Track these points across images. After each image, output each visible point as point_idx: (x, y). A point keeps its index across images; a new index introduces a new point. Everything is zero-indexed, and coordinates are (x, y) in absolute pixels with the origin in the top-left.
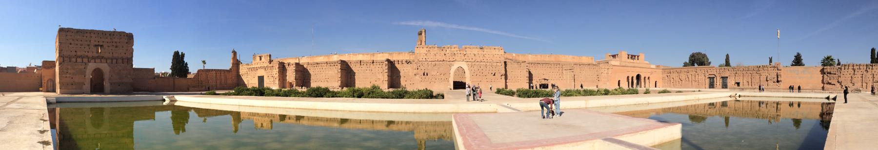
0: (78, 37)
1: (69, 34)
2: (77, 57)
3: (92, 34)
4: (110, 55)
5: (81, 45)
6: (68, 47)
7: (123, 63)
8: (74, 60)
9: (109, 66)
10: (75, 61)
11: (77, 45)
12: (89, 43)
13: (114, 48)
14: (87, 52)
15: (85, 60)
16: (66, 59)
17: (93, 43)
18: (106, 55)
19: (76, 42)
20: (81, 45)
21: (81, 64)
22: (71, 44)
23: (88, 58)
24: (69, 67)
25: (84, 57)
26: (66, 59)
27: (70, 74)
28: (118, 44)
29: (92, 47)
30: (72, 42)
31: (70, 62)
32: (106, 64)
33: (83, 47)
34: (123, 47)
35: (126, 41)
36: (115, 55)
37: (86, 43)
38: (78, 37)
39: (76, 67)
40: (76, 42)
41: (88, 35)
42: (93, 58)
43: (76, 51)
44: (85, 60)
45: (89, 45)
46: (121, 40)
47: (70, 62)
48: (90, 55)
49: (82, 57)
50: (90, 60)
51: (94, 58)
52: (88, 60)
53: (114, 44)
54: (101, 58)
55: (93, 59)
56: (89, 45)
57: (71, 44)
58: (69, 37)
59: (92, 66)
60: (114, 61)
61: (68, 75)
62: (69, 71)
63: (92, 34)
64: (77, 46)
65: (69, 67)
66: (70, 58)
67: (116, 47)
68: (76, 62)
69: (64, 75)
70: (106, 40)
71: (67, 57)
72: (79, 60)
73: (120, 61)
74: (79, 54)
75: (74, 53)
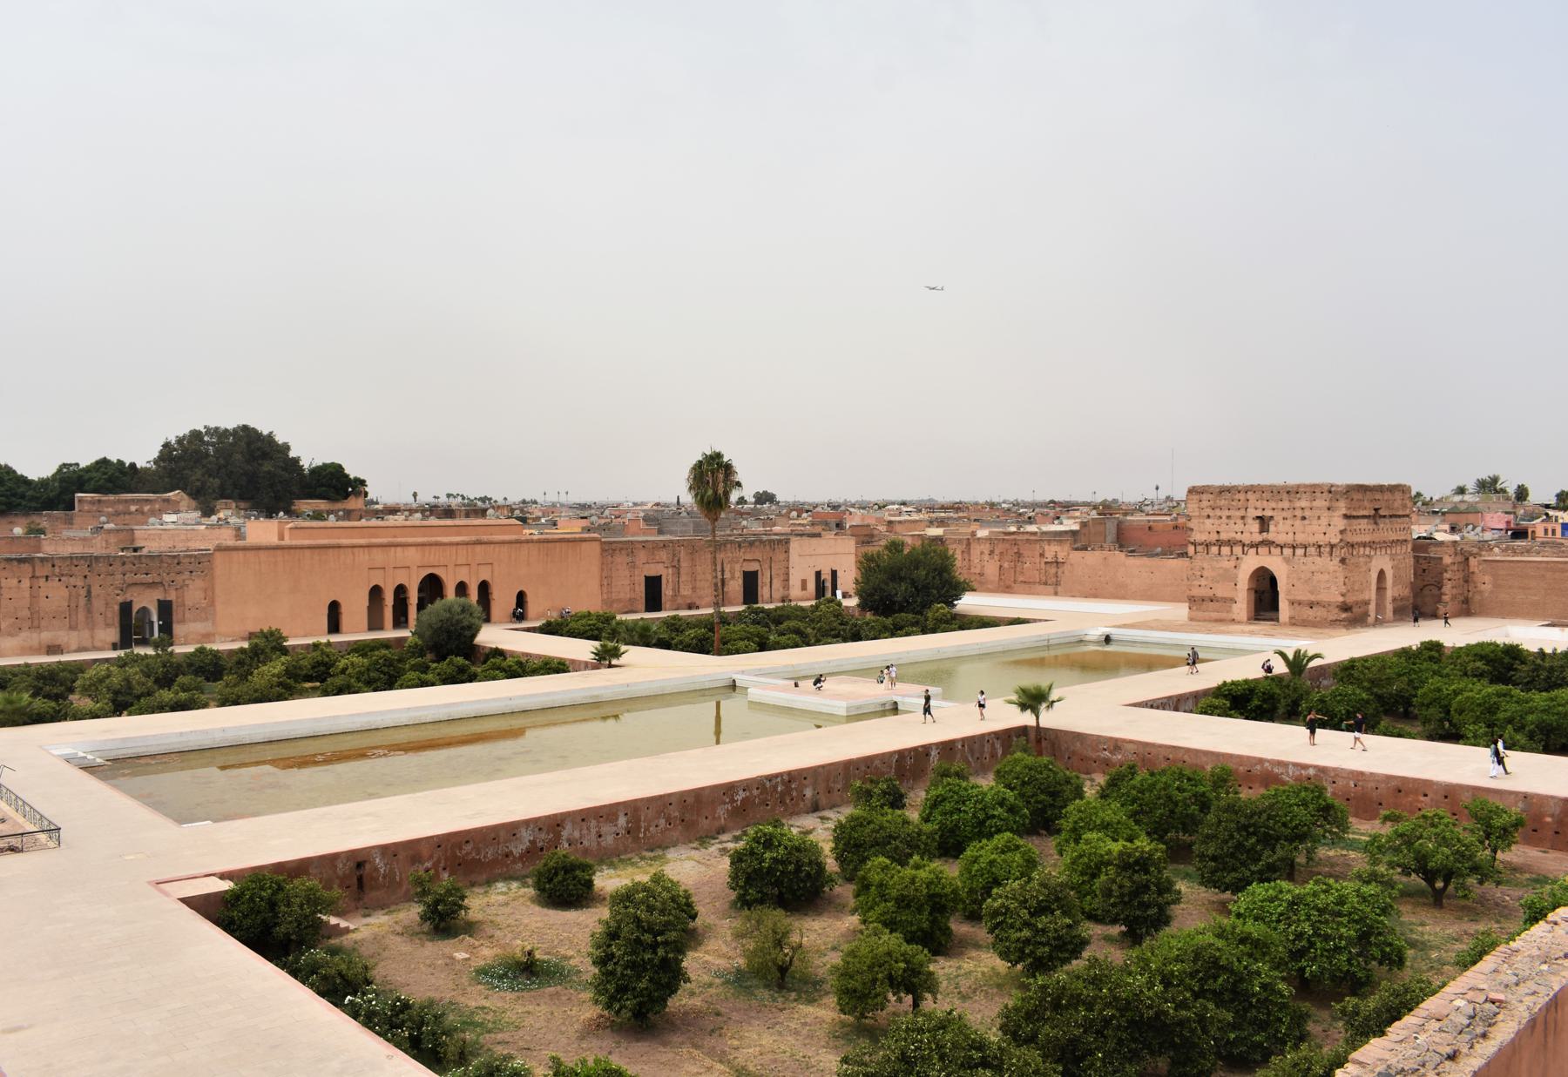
0: (1223, 502)
1: (1204, 497)
2: (1220, 543)
3: (1250, 495)
4: (1289, 539)
7: (1320, 556)
8: (1214, 549)
9: (1287, 560)
12: (1242, 513)
13: (1298, 523)
15: (1238, 550)
16: (1199, 548)
17: (1252, 513)
18: (1281, 539)
19: (1218, 512)
20: (1229, 517)
22: (1209, 517)
23: (1244, 545)
28: (1307, 513)
32: (1280, 558)
33: (1232, 522)
34: (1319, 518)
35: (1327, 504)
36: (1300, 538)
38: (1223, 502)
41: (1242, 496)
42: (1252, 546)
43: (1218, 532)
44: (1238, 550)
46: (1315, 504)
48: (1246, 539)
49: (1231, 543)
50: (1246, 549)
51: (1255, 545)
53: (1299, 513)
54: (1268, 544)
56: (1243, 518)
57: (1209, 517)
59: (1251, 562)
60: (1300, 552)
61: (1203, 582)
62: (1205, 574)
63: (1250, 495)
64: (1219, 521)
66: (1208, 545)
67: (1304, 518)
70: (1281, 505)
72: (1225, 550)
73: (1312, 550)
74: (1224, 536)
75: (1214, 537)
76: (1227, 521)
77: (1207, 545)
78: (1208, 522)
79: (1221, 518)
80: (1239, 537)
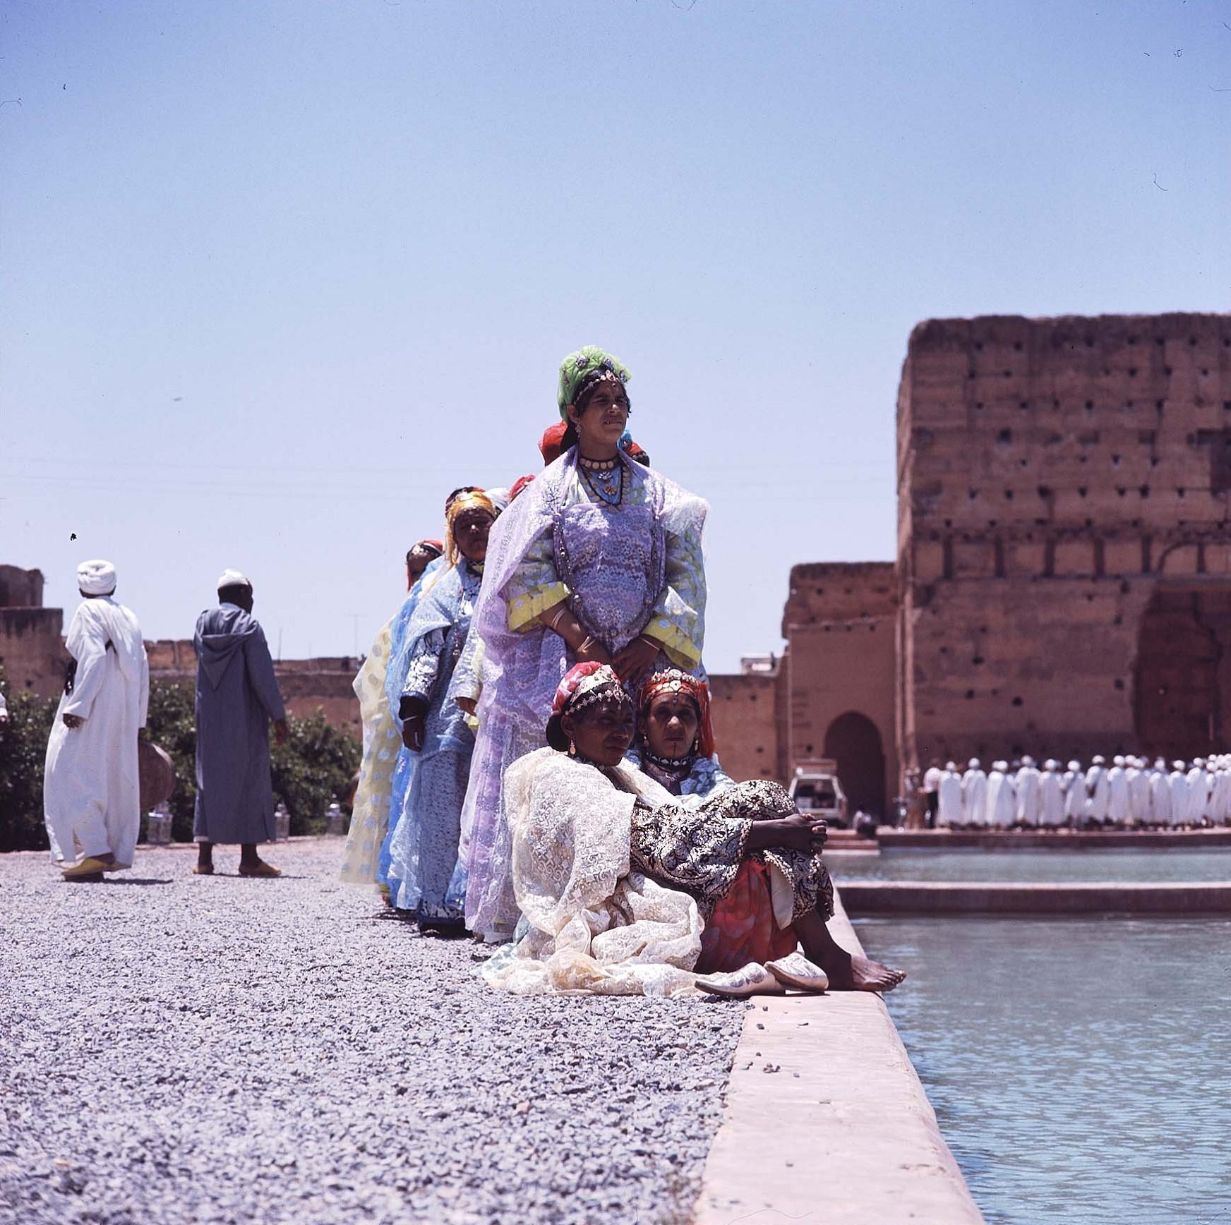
1: (989, 359)
5: (1092, 438)
6: (987, 457)
8: (1029, 556)
10: (1039, 568)
11: (1055, 438)
14: (1132, 498)
16: (964, 552)
19: (1049, 421)
20: (1092, 438)
21: (1088, 586)
23: (1147, 541)
24: (993, 615)
25: (1112, 533)
26: (964, 552)
27: (1001, 666)
29: (1179, 449)
30: (1018, 421)
31: (1000, 573)
37: (1129, 420)
39: (1044, 617)
40: (1049, 421)
41: (1142, 357)
43: (1044, 492)
45: (1149, 438)
47: (1000, 573)
50: (1157, 551)
52: (1146, 558)
55: (1185, 541)
56: (1149, 438)
57: (1005, 435)
58: (989, 386)
61: (984, 681)
62: (993, 647)
63: (1175, 352)
65: (993, 615)
68: (1049, 573)
69: (957, 684)
71: (980, 538)
72: (1075, 555)
74: (1069, 507)
76: (1078, 449)
77: (998, 543)
78: (1005, 452)
79: (1055, 438)
80: (1130, 505)
